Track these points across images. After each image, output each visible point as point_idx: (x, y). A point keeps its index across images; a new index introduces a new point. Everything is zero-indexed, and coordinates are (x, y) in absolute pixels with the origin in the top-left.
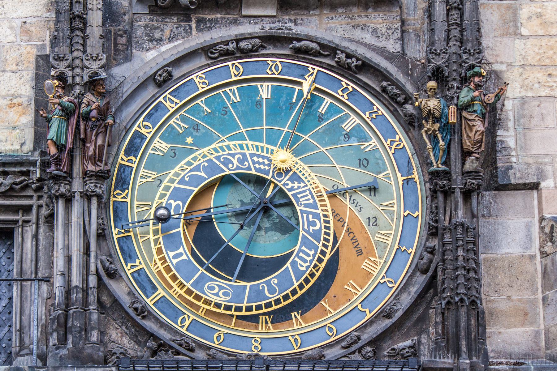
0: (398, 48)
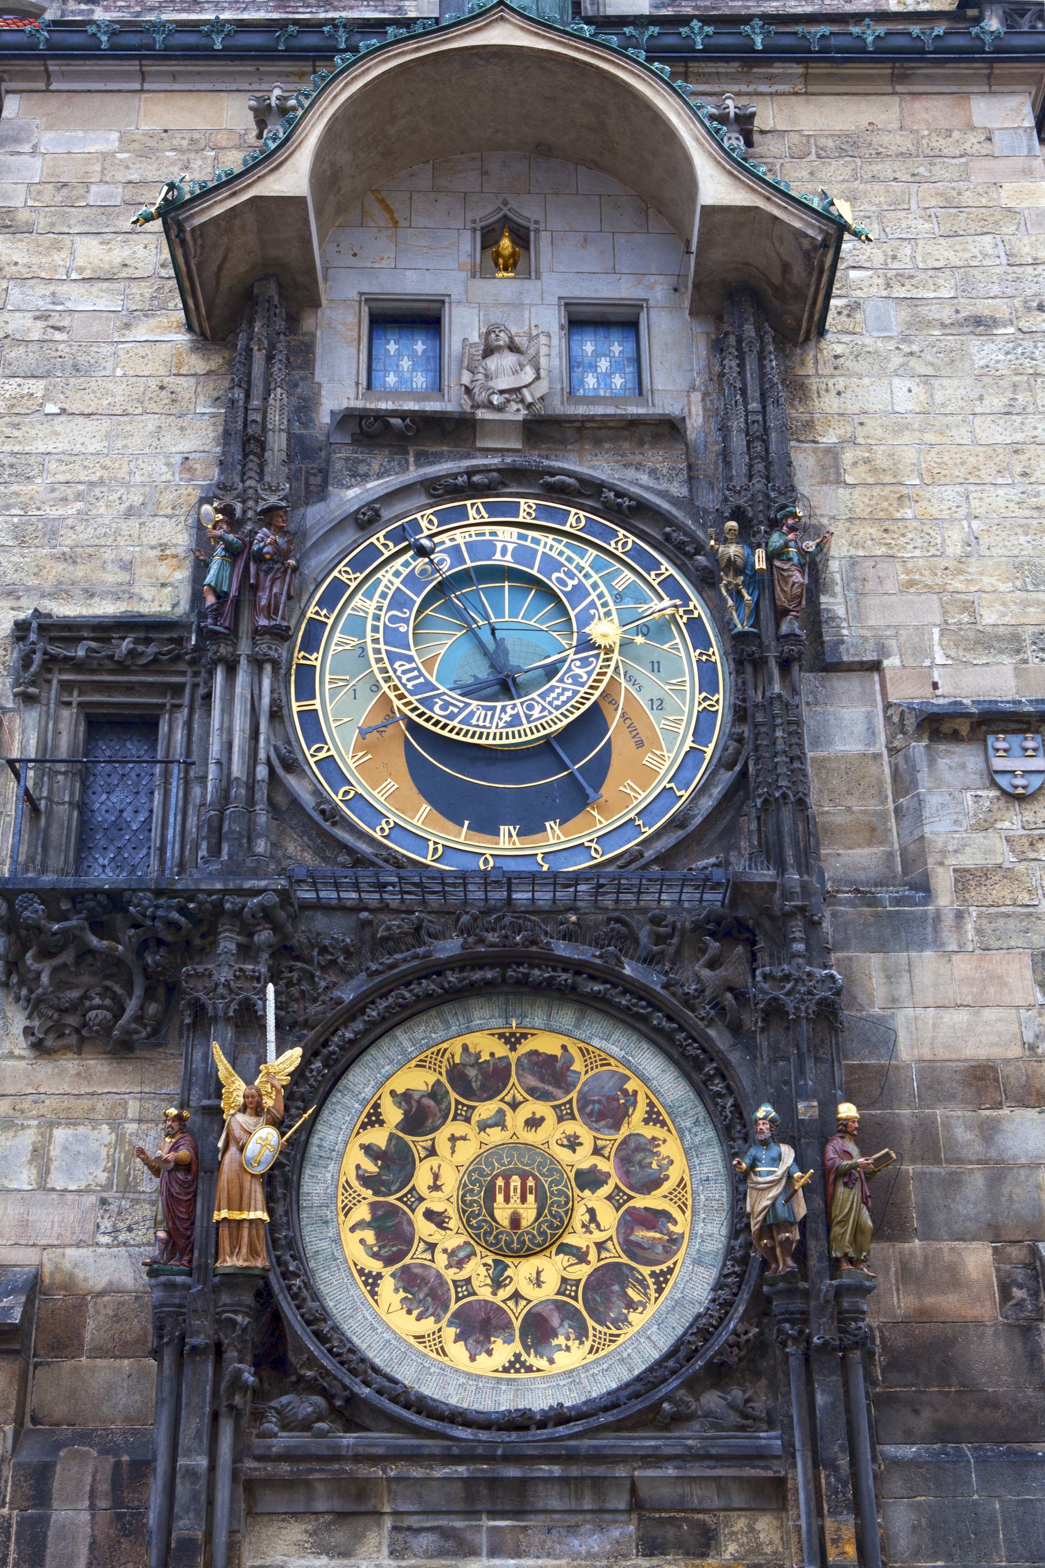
0: (684, 491)
